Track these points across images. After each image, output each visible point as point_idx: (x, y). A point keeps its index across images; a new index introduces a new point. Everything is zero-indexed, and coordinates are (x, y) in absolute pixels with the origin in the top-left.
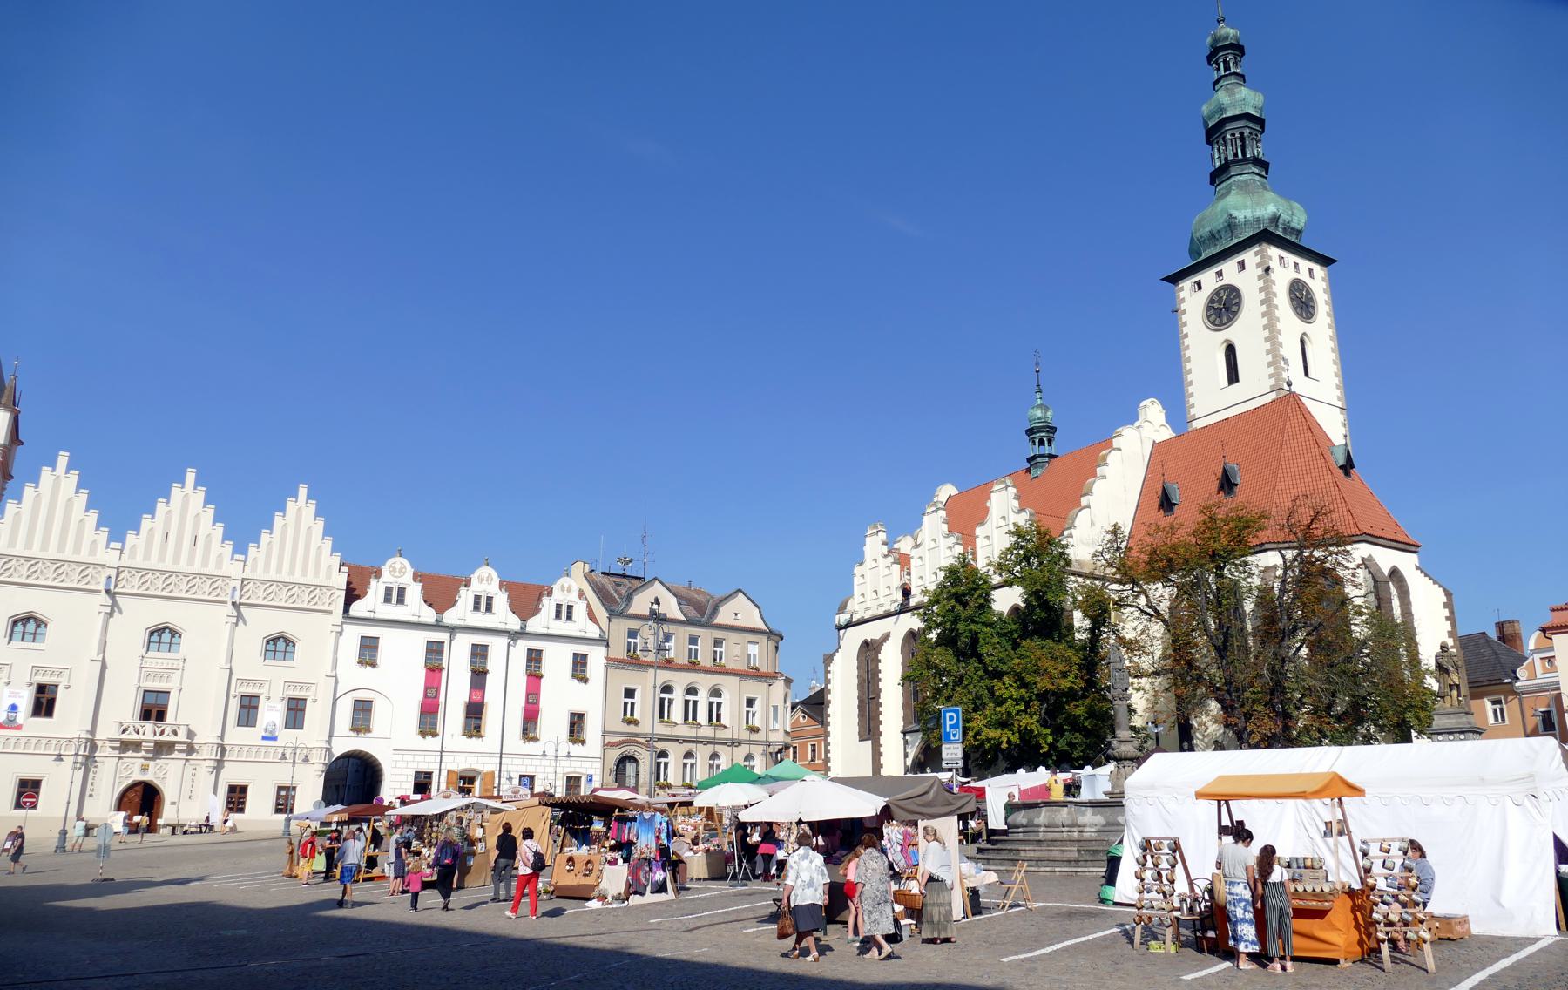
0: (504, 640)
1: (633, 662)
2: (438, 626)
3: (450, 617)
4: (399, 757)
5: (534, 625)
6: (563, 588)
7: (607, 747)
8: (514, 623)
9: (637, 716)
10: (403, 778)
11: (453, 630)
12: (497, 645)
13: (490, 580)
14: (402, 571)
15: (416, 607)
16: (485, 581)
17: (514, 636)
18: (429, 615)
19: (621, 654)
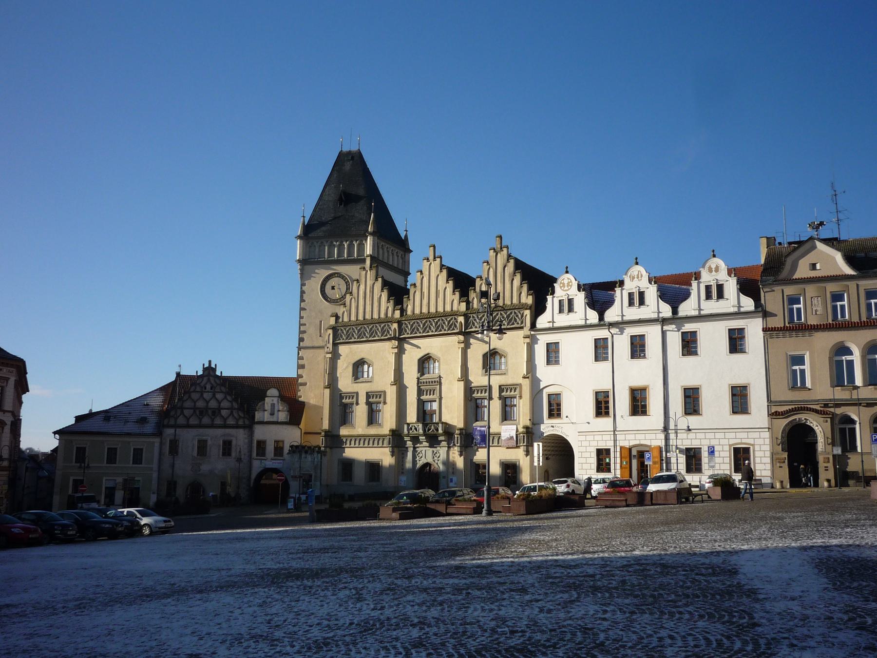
0: (656, 329)
1: (797, 328)
2: (602, 323)
3: (611, 315)
4: (583, 438)
5: (687, 308)
6: (710, 270)
7: (774, 415)
8: (666, 311)
9: (808, 384)
10: (588, 455)
11: (611, 325)
12: (652, 334)
13: (639, 276)
14: (569, 285)
15: (583, 313)
16: (638, 279)
17: (664, 321)
18: (593, 316)
19: (777, 322)
